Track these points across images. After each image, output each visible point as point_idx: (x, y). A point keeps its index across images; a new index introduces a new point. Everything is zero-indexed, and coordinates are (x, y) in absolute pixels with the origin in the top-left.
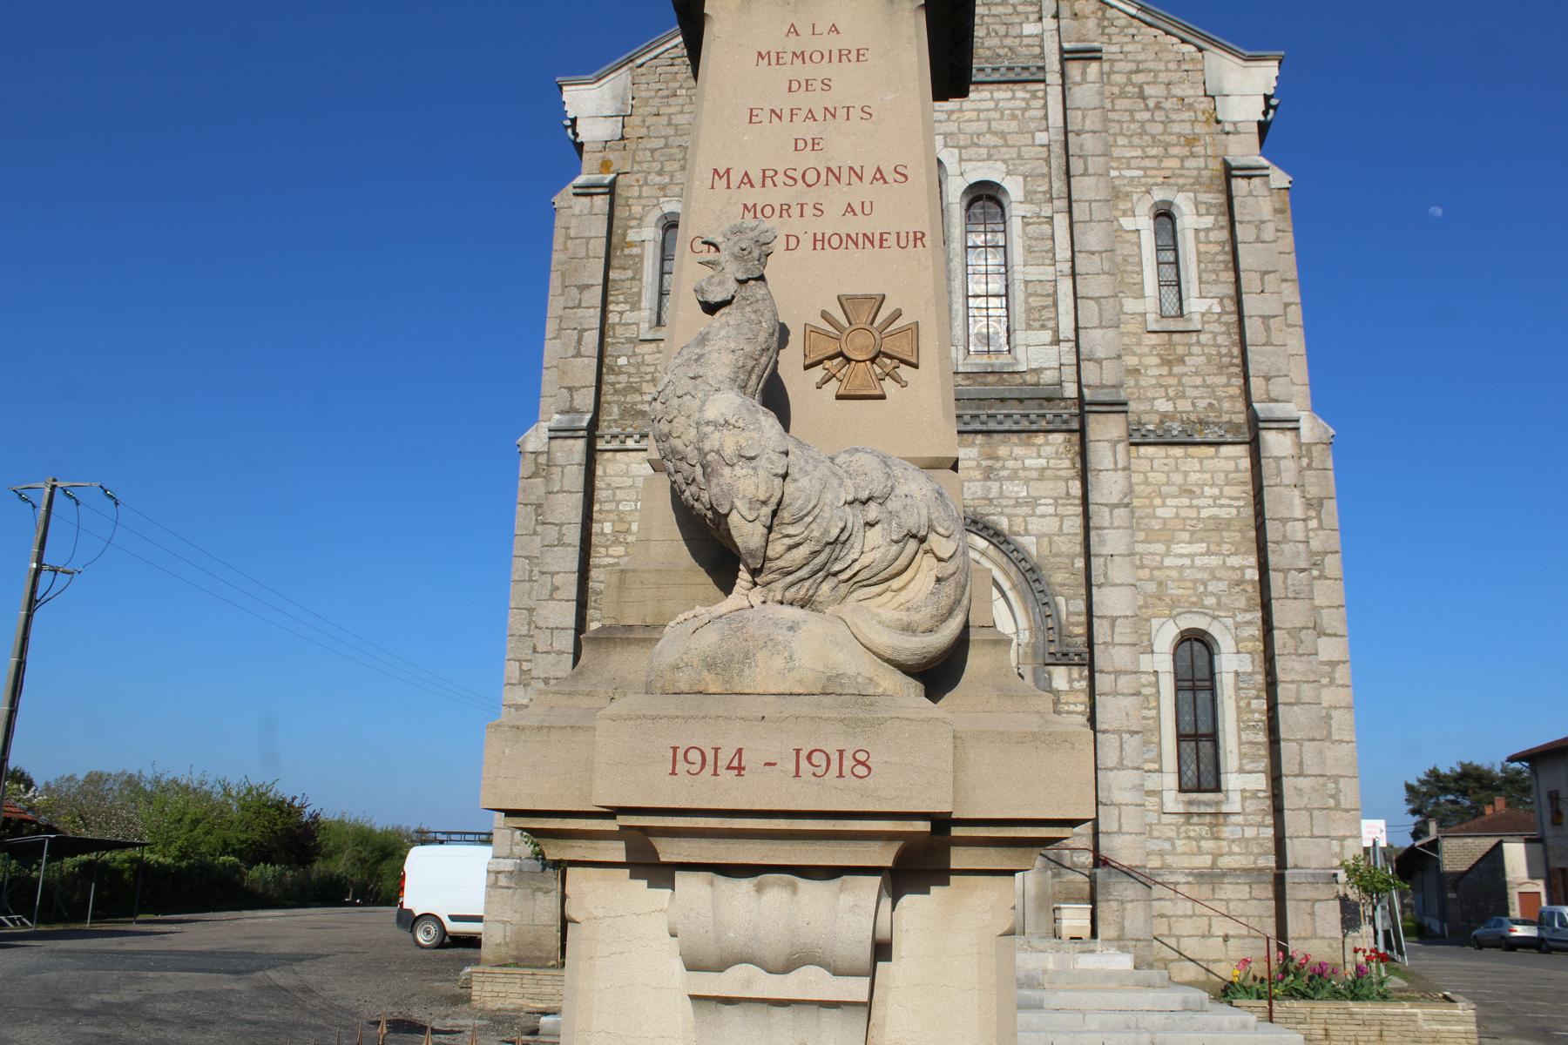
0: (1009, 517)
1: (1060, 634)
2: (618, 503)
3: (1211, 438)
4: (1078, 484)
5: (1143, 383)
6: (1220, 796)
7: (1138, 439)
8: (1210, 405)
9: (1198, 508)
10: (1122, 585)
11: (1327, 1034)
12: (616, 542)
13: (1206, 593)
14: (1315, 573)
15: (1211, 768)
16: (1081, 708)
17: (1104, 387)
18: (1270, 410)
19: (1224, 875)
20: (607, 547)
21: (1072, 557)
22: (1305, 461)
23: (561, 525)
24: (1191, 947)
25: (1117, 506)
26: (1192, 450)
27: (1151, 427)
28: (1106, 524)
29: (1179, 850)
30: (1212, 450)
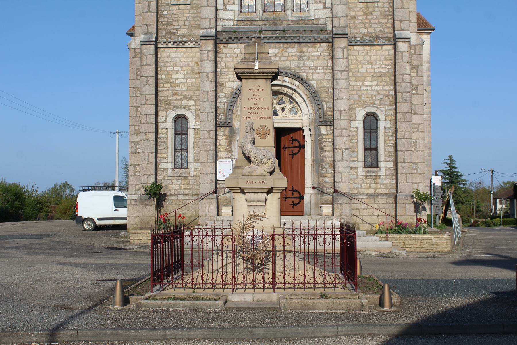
0: (307, 73)
1: (324, 115)
2: (167, 67)
3: (380, 43)
4: (331, 61)
5: (356, 22)
6: (378, 169)
7: (353, 43)
8: (381, 30)
9: (374, 69)
10: (344, 99)
11: (404, 244)
12: (167, 82)
13: (376, 99)
14: (414, 92)
15: (375, 159)
16: (330, 140)
17: (340, 27)
18: (401, 34)
19: (378, 195)
20: (163, 84)
21: (328, 88)
22: (413, 52)
23: (147, 77)
24: (366, 218)
25: (343, 71)
26: (373, 47)
27: (358, 39)
28: (339, 78)
29: (363, 187)
30: (380, 47)
